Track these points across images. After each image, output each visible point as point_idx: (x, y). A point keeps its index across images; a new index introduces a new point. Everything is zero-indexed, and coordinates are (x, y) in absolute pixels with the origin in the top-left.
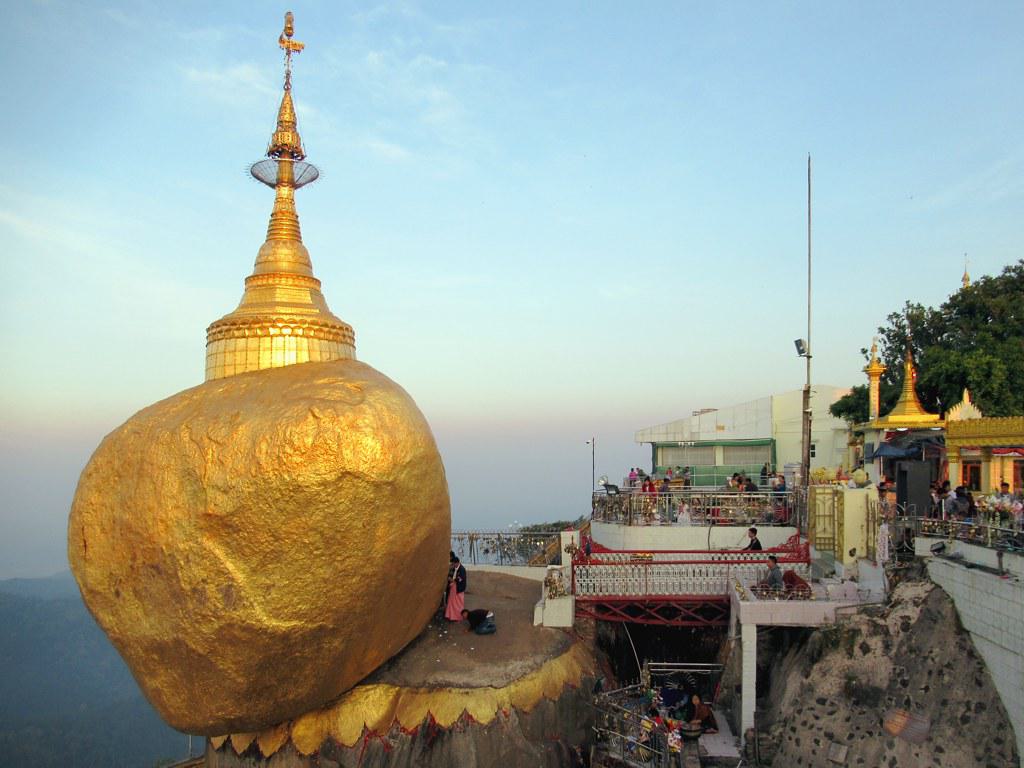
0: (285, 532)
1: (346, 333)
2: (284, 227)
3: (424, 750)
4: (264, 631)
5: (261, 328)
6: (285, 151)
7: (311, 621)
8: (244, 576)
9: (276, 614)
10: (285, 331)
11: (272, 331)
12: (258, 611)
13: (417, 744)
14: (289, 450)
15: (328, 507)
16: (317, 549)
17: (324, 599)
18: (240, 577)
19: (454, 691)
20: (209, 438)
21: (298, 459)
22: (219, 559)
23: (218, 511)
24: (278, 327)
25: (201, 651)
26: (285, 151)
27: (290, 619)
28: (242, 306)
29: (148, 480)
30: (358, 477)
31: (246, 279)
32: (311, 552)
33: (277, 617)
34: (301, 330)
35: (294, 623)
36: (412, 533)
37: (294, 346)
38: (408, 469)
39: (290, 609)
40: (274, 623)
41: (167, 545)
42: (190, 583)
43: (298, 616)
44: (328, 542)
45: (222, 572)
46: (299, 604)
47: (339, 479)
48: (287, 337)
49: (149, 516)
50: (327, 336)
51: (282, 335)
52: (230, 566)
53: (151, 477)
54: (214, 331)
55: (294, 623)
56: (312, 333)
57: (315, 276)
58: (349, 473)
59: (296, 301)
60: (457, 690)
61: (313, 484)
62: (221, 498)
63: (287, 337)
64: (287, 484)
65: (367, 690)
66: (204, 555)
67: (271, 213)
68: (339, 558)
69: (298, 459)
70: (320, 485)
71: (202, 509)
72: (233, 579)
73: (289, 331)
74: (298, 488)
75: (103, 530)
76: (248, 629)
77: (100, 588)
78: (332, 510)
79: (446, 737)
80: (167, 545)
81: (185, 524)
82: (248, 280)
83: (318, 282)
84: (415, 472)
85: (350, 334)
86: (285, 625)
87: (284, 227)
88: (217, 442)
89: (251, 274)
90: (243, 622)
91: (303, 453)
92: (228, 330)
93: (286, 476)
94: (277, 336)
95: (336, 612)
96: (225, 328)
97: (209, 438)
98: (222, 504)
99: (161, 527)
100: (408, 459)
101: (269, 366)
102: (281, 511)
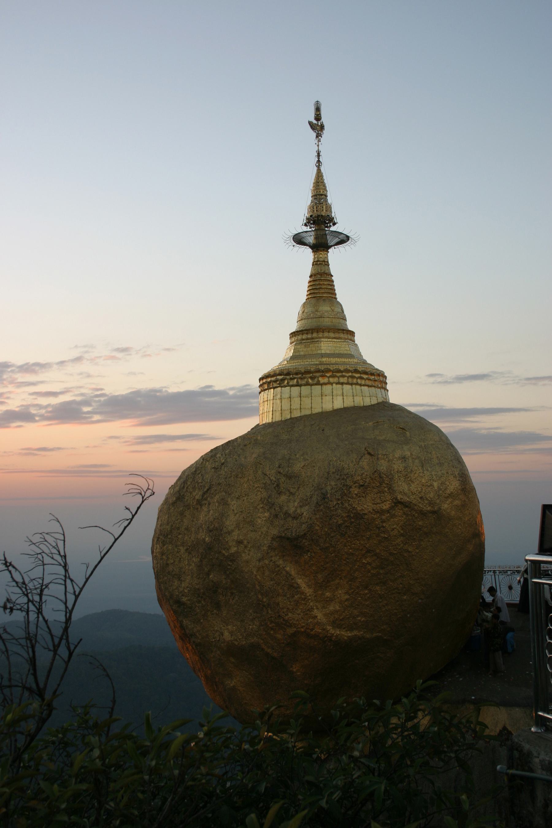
1: (376, 378)
2: (321, 285)
5: (312, 378)
8: (311, 590)
9: (336, 624)
10: (331, 380)
11: (322, 380)
22: (291, 575)
24: (326, 376)
25: (275, 655)
27: (351, 629)
28: (293, 358)
30: (407, 507)
31: (290, 335)
33: (340, 627)
34: (346, 378)
35: (355, 633)
37: (340, 392)
38: (450, 500)
46: (358, 616)
47: (392, 508)
48: (334, 385)
50: (368, 382)
54: (269, 380)
55: (355, 633)
56: (355, 381)
57: (350, 328)
58: (401, 503)
59: (337, 352)
61: (370, 512)
63: (334, 385)
67: (309, 275)
73: (336, 380)
77: (184, 599)
82: (293, 335)
83: (352, 333)
84: (457, 502)
85: (381, 379)
86: (346, 634)
87: (321, 285)
89: (294, 330)
91: (362, 486)
92: (283, 380)
94: (325, 384)
96: (280, 377)
101: (320, 410)
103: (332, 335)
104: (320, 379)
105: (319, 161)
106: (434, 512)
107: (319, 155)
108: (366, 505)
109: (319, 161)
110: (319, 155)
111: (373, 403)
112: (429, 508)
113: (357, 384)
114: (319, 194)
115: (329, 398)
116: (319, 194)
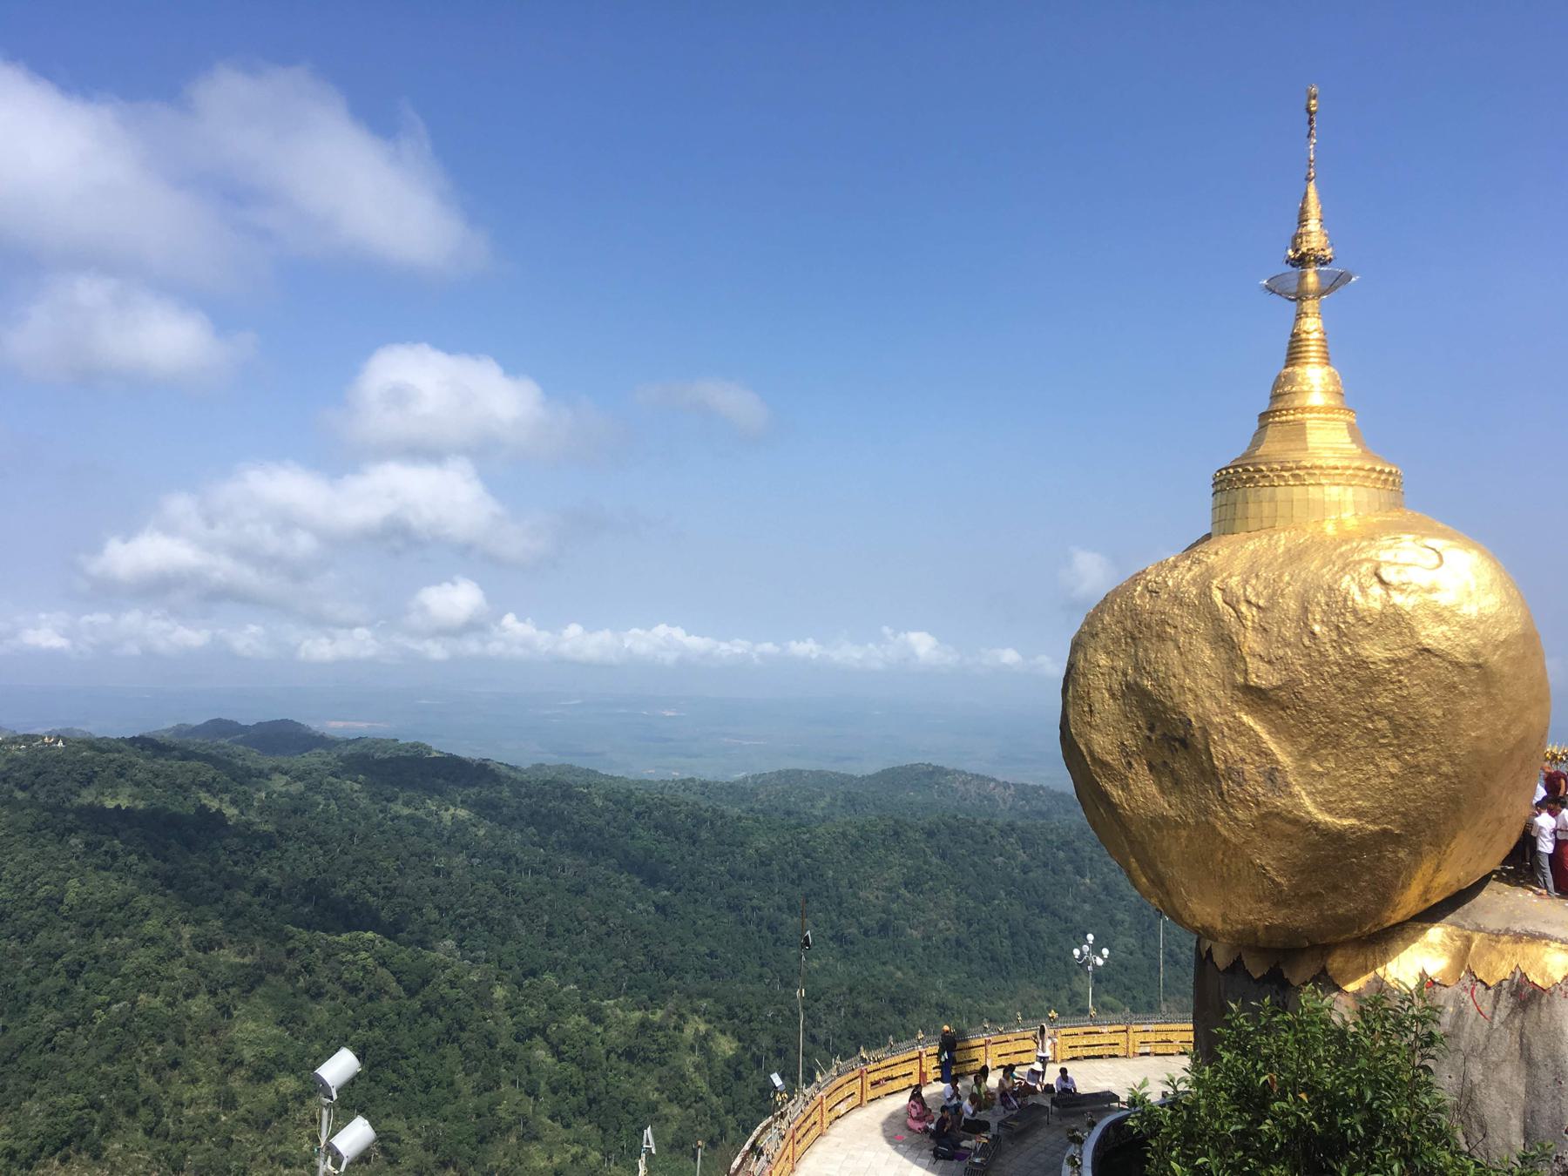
0: (1344, 714)
3: (1513, 1011)
4: (1316, 826)
7: (1374, 822)
12: (1307, 802)
13: (1502, 1003)
14: (1350, 618)
16: (1384, 737)
17: (1389, 797)
18: (1284, 759)
19: (1553, 945)
20: (1249, 602)
21: (1363, 631)
23: (1263, 684)
27: (1347, 816)
29: (1170, 644)
32: (1376, 740)
33: (1330, 811)
36: (1506, 730)
39: (1347, 805)
41: (1197, 716)
42: (1226, 761)
43: (1357, 813)
44: (1397, 729)
45: (1265, 753)
49: (1173, 682)
52: (1273, 746)
53: (1176, 641)
60: (1558, 945)
62: (1264, 667)
64: (1349, 658)
66: (1240, 730)
69: (1363, 631)
70: (1390, 661)
71: (1240, 679)
72: (1278, 762)
74: (1363, 664)
75: (1113, 696)
76: (1296, 822)
77: (1109, 758)
78: (1405, 693)
79: (1544, 1001)
80: (1197, 716)
81: (1219, 693)
84: (1511, 653)
88: (1259, 607)
93: (1347, 649)
95: (1404, 815)
97: (1249, 602)
98: (1262, 676)
99: (1190, 697)
100: (1501, 638)
102: (1340, 689)
106: (1478, 666)
108: (1375, 651)
112: (1472, 660)
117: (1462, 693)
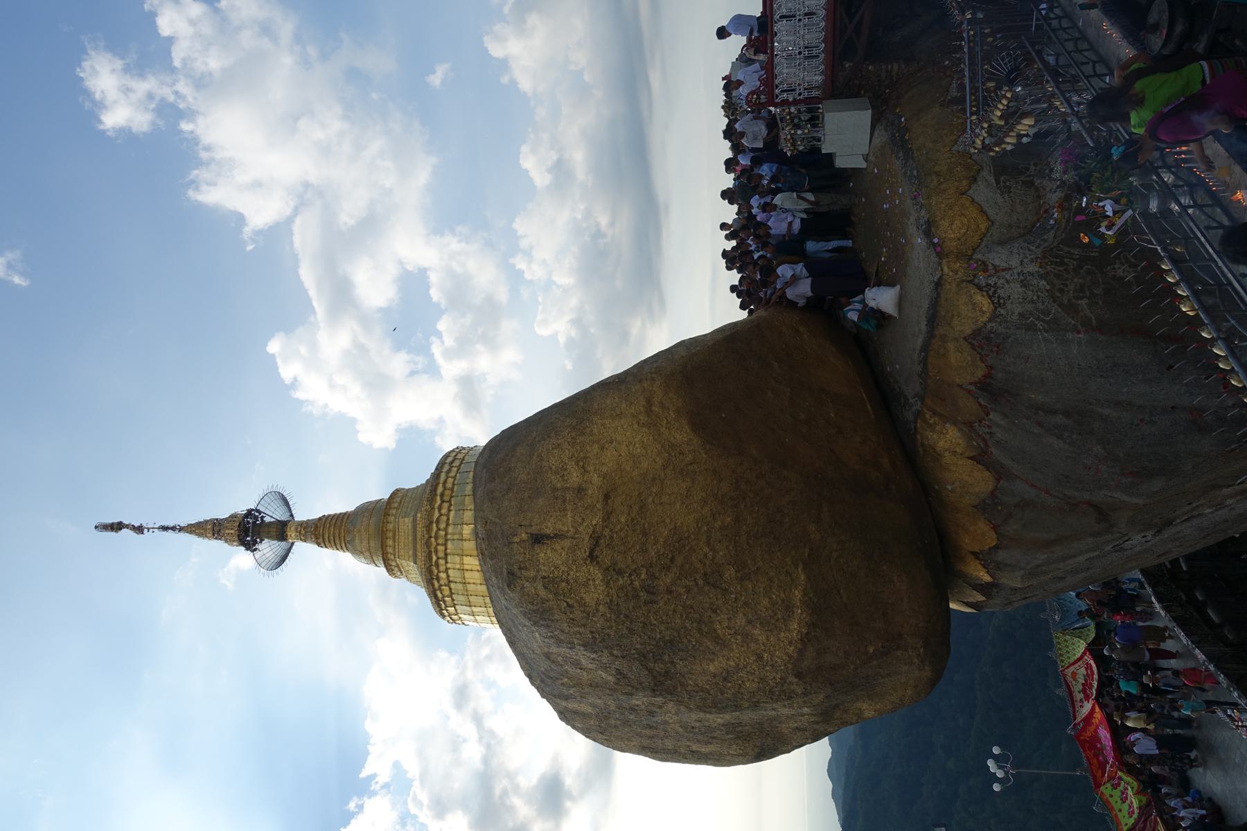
6: (247, 530)
10: (442, 568)
15: (639, 575)
26: (247, 530)
37: (457, 559)
40: (794, 626)
51: (447, 570)
65: (923, 445)
68: (710, 555)
73: (442, 562)
76: (801, 653)
90: (790, 657)
94: (448, 576)
103: (390, 542)
104: (442, 582)
105: (173, 528)
107: (165, 528)
109: (173, 528)
110: (165, 528)
111: (472, 507)
112: (599, 506)
113: (446, 529)
114: (213, 529)
115: (467, 574)
116: (213, 529)
117: (641, 508)
